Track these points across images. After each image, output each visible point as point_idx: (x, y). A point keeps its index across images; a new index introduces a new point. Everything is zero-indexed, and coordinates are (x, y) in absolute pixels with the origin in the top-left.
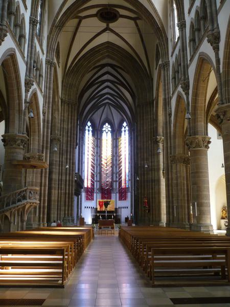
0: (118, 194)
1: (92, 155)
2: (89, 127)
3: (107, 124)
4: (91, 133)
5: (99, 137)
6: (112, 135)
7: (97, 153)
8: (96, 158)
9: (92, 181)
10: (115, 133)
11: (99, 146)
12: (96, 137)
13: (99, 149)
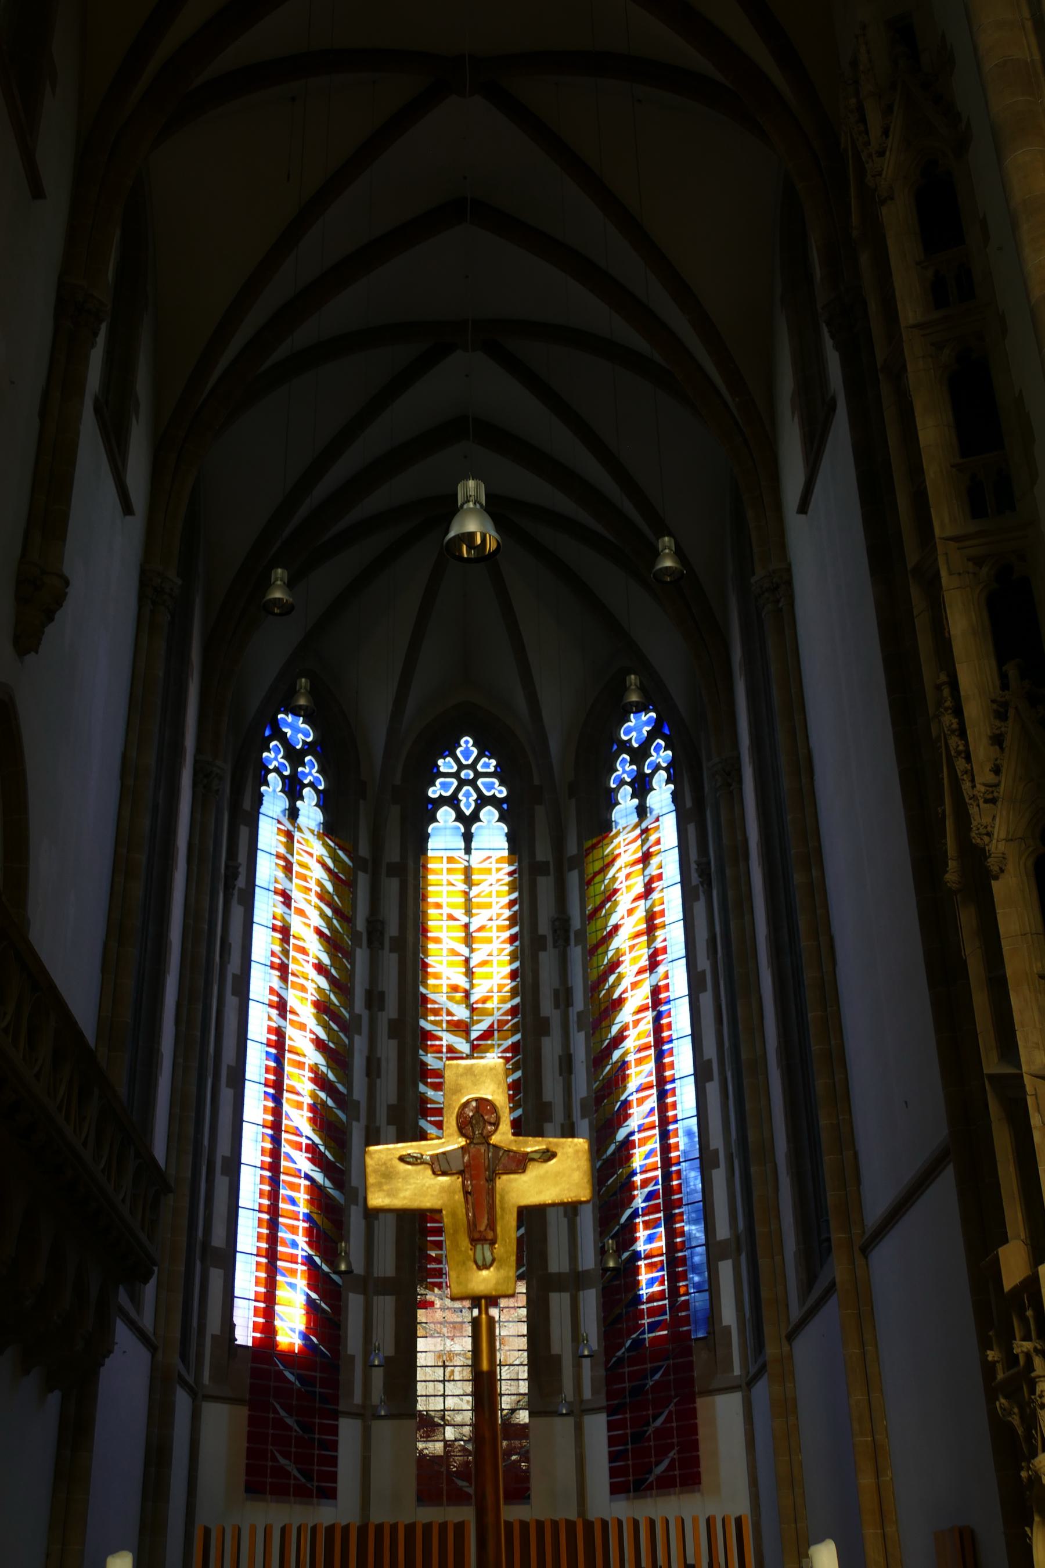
0: (597, 1426)
1: (322, 1007)
2: (295, 757)
3: (467, 742)
4: (310, 814)
5: (392, 854)
6: (510, 837)
7: (375, 999)
8: (360, 1043)
9: (316, 1278)
10: (541, 813)
11: (392, 929)
12: (364, 851)
13: (390, 961)
